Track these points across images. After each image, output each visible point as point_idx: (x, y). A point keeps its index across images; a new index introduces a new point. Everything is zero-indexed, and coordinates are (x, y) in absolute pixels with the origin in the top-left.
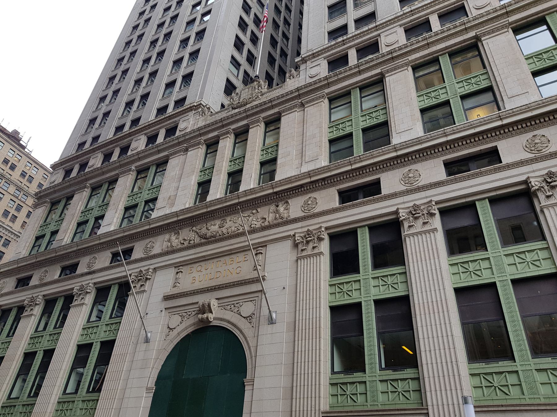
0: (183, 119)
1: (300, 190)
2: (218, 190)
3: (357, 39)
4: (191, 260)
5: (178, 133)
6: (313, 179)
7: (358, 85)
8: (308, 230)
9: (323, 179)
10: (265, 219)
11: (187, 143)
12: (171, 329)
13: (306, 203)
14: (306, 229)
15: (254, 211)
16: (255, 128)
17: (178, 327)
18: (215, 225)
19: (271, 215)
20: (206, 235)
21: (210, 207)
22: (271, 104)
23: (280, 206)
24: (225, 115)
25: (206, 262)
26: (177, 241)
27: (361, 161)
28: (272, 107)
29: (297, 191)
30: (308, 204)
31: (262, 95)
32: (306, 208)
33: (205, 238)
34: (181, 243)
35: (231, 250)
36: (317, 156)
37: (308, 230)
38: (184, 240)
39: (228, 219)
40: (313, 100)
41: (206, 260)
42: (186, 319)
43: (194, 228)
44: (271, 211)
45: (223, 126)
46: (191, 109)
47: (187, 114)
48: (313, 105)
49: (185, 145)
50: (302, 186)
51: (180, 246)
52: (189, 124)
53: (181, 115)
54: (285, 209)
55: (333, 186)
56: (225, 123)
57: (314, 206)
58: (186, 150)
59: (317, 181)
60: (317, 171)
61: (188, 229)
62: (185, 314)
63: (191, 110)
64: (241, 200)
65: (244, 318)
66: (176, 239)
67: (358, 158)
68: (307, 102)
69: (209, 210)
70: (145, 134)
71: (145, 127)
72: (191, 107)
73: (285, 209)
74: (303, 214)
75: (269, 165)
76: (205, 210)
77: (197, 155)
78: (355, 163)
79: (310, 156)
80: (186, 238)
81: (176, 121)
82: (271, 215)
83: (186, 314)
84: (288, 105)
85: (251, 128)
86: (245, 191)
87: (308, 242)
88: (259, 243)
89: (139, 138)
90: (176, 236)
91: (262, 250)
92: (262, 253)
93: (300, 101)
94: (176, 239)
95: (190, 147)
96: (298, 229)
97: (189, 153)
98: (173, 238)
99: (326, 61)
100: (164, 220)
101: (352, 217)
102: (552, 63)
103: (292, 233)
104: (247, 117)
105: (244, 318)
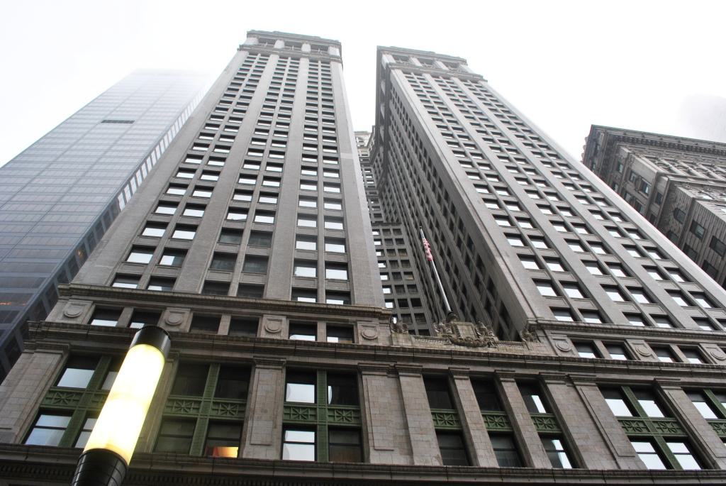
21: (507, 477)
22: (490, 360)
27: (709, 478)
47: (370, 319)
49: (392, 364)
63: (375, 317)
81: (348, 321)
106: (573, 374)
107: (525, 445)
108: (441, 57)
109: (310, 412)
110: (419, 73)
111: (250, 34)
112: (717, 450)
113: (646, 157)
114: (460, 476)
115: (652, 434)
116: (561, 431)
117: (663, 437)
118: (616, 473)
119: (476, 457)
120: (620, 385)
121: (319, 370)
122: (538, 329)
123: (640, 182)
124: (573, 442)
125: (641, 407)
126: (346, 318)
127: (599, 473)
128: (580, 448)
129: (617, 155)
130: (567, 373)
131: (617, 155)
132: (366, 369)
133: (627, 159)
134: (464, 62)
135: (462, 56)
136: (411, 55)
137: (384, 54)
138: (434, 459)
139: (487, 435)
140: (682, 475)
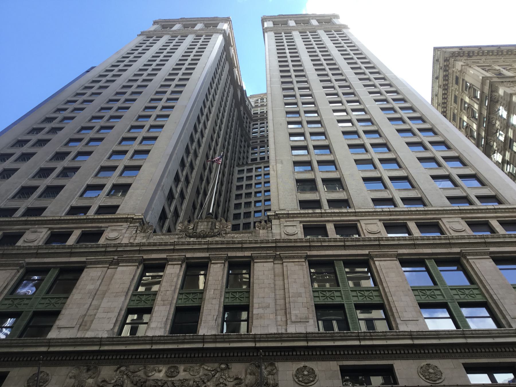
0: (113, 228)
1: (290, 353)
2: (157, 325)
3: (335, 216)
5: (102, 241)
6: (311, 344)
7: (342, 258)
11: (116, 256)
13: (299, 371)
15: (223, 366)
16: (219, 265)
18: (160, 371)
20: (145, 382)
23: (263, 367)
24: (176, 240)
28: (242, 249)
29: (287, 354)
30: (304, 375)
31: (226, 234)
32: (301, 379)
36: (306, 318)
38: (104, 381)
39: (181, 368)
40: (293, 257)
43: (123, 368)
45: (174, 250)
46: (126, 220)
48: (299, 262)
49: (116, 257)
52: (116, 234)
53: (110, 222)
54: (270, 373)
55: (334, 359)
56: (177, 247)
57: (311, 379)
58: (116, 263)
60: (316, 335)
61: (115, 367)
63: (127, 222)
64: (207, 345)
67: (368, 334)
68: (286, 258)
69: (155, 347)
70: (50, 229)
71: (52, 220)
72: (127, 218)
73: (270, 373)
75: (235, 311)
76: (148, 347)
77: (125, 274)
78: (365, 339)
79: (296, 316)
81: (101, 227)
82: (249, 376)
84: (264, 253)
85: (213, 263)
89: (39, 230)
90: (90, 373)
93: (278, 253)
94: (90, 377)
95: (123, 261)
97: (120, 269)
98: (85, 375)
99: (302, 225)
102: (434, 301)
104: (208, 250)
106: (283, 253)
108: (314, 17)
109: (26, 302)
110: (287, 31)
111: (155, 23)
112: (405, 314)
113: (478, 66)
114: (113, 345)
118: (268, 336)
120: (333, 260)
121: (54, 268)
122: (275, 219)
123: (473, 89)
126: (100, 225)
129: (454, 69)
130: (278, 253)
131: (454, 69)
132: (91, 263)
133: (461, 71)
134: (337, 17)
135: (336, 13)
136: (289, 19)
137: (266, 21)
138: (106, 332)
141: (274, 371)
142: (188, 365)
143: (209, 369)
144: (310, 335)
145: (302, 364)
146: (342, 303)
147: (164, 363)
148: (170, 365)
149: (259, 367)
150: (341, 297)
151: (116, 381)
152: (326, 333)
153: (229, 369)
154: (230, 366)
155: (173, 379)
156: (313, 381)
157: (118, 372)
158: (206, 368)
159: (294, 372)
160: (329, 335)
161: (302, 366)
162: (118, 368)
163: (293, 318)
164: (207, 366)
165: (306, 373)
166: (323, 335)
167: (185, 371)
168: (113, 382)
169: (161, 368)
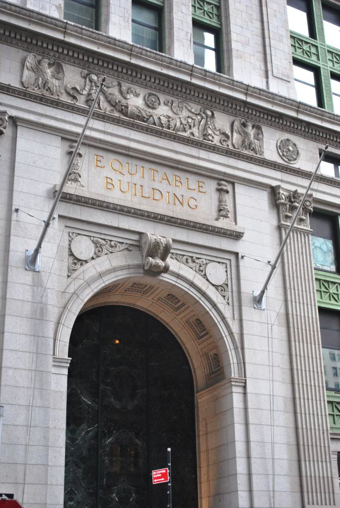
4: (101, 141)
8: (296, 192)
9: (309, 124)
10: (227, 136)
12: (79, 260)
14: (293, 188)
17: (93, 262)
19: (235, 134)
21: (137, 57)
25: (130, 160)
26: (56, 83)
32: (285, 154)
33: (121, 112)
34: (68, 94)
35: (179, 162)
37: (296, 192)
38: (74, 89)
41: (127, 156)
42: (105, 251)
44: (235, 128)
50: (281, 116)
51: (65, 98)
57: (295, 157)
59: (302, 121)
60: (309, 108)
62: (103, 242)
65: (213, 285)
66: (53, 76)
74: (280, 161)
80: (78, 88)
83: (103, 242)
86: (248, 86)
87: (293, 208)
88: (225, 174)
91: (229, 188)
92: (227, 192)
96: (288, 184)
98: (49, 72)
100: (30, 22)
101: (329, 196)
103: (274, 183)
105: (213, 285)
107: (171, 28)
114: (81, 39)
115: (320, 64)
116: (221, 25)
117: (331, 71)
118: (262, 92)
119: (107, 21)
124: (229, 42)
125: (322, 29)
127: (244, 86)
128: (234, 53)
138: (54, 8)
139: (191, 23)
140: (330, 118)
141: (260, 136)
142: (170, 98)
143: (193, 110)
144: (303, 106)
145: (286, 136)
146: (319, 65)
147: (146, 87)
148: (151, 92)
149: (244, 125)
150: (318, 56)
151: (89, 94)
152: (318, 110)
153: (214, 118)
154: (216, 115)
155: (151, 110)
156: (295, 159)
157: (87, 80)
158: (190, 108)
159: (279, 144)
160: (320, 112)
161: (286, 138)
162: (88, 74)
163: (275, 71)
164: (189, 105)
165: (291, 148)
166: (315, 110)
167: (165, 104)
168: (85, 92)
169: (138, 91)
